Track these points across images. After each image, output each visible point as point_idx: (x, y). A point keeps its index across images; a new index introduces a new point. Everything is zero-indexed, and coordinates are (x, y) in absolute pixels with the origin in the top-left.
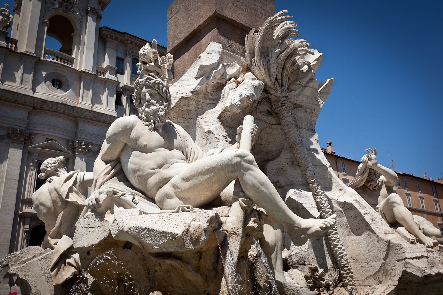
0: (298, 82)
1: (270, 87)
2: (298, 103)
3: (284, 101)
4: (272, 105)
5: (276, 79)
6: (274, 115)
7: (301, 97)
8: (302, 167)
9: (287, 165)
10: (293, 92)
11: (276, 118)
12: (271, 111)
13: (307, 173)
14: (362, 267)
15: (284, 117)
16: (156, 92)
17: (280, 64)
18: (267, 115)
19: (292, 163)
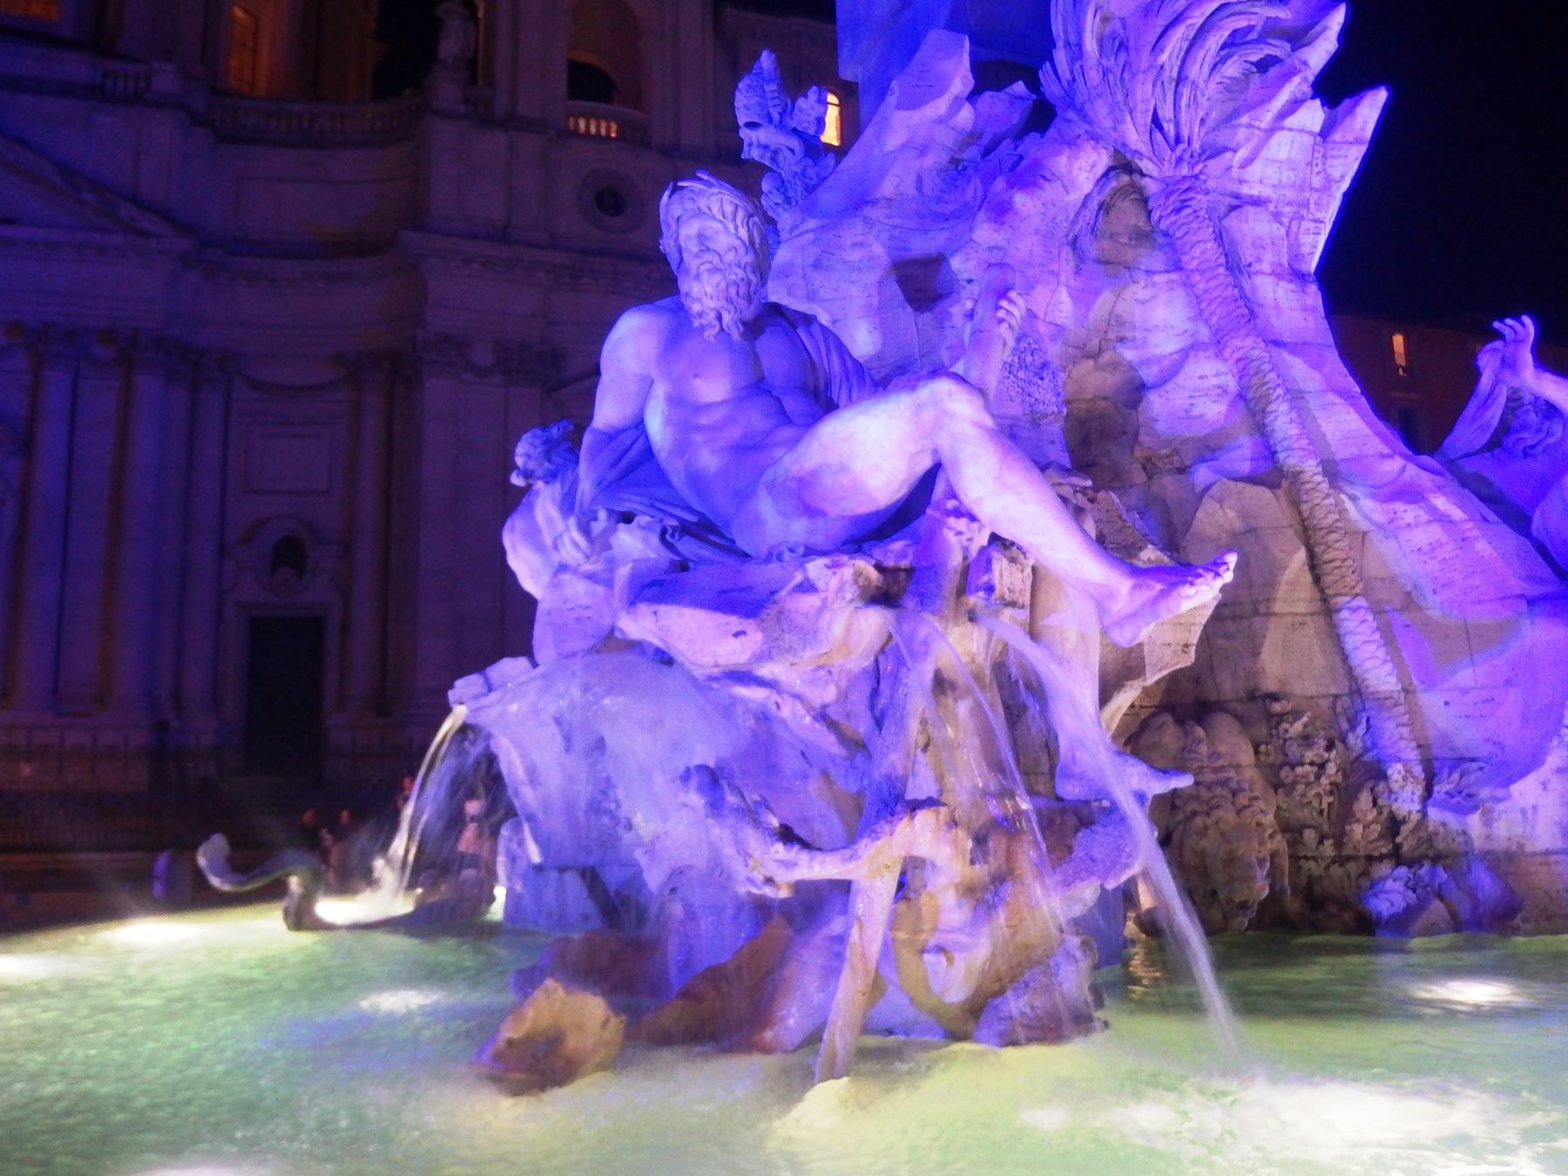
0: (1244, 120)
1: (1137, 152)
2: (1245, 190)
3: (1186, 190)
4: (1150, 208)
5: (1156, 121)
6: (1161, 240)
7: (1256, 169)
8: (1251, 400)
9: (1205, 399)
10: (1228, 155)
11: (1167, 249)
12: (1148, 229)
13: (1266, 421)
14: (1447, 704)
15: (1188, 246)
16: (718, 226)
17: (1167, 68)
18: (1133, 242)
19: (1220, 390)
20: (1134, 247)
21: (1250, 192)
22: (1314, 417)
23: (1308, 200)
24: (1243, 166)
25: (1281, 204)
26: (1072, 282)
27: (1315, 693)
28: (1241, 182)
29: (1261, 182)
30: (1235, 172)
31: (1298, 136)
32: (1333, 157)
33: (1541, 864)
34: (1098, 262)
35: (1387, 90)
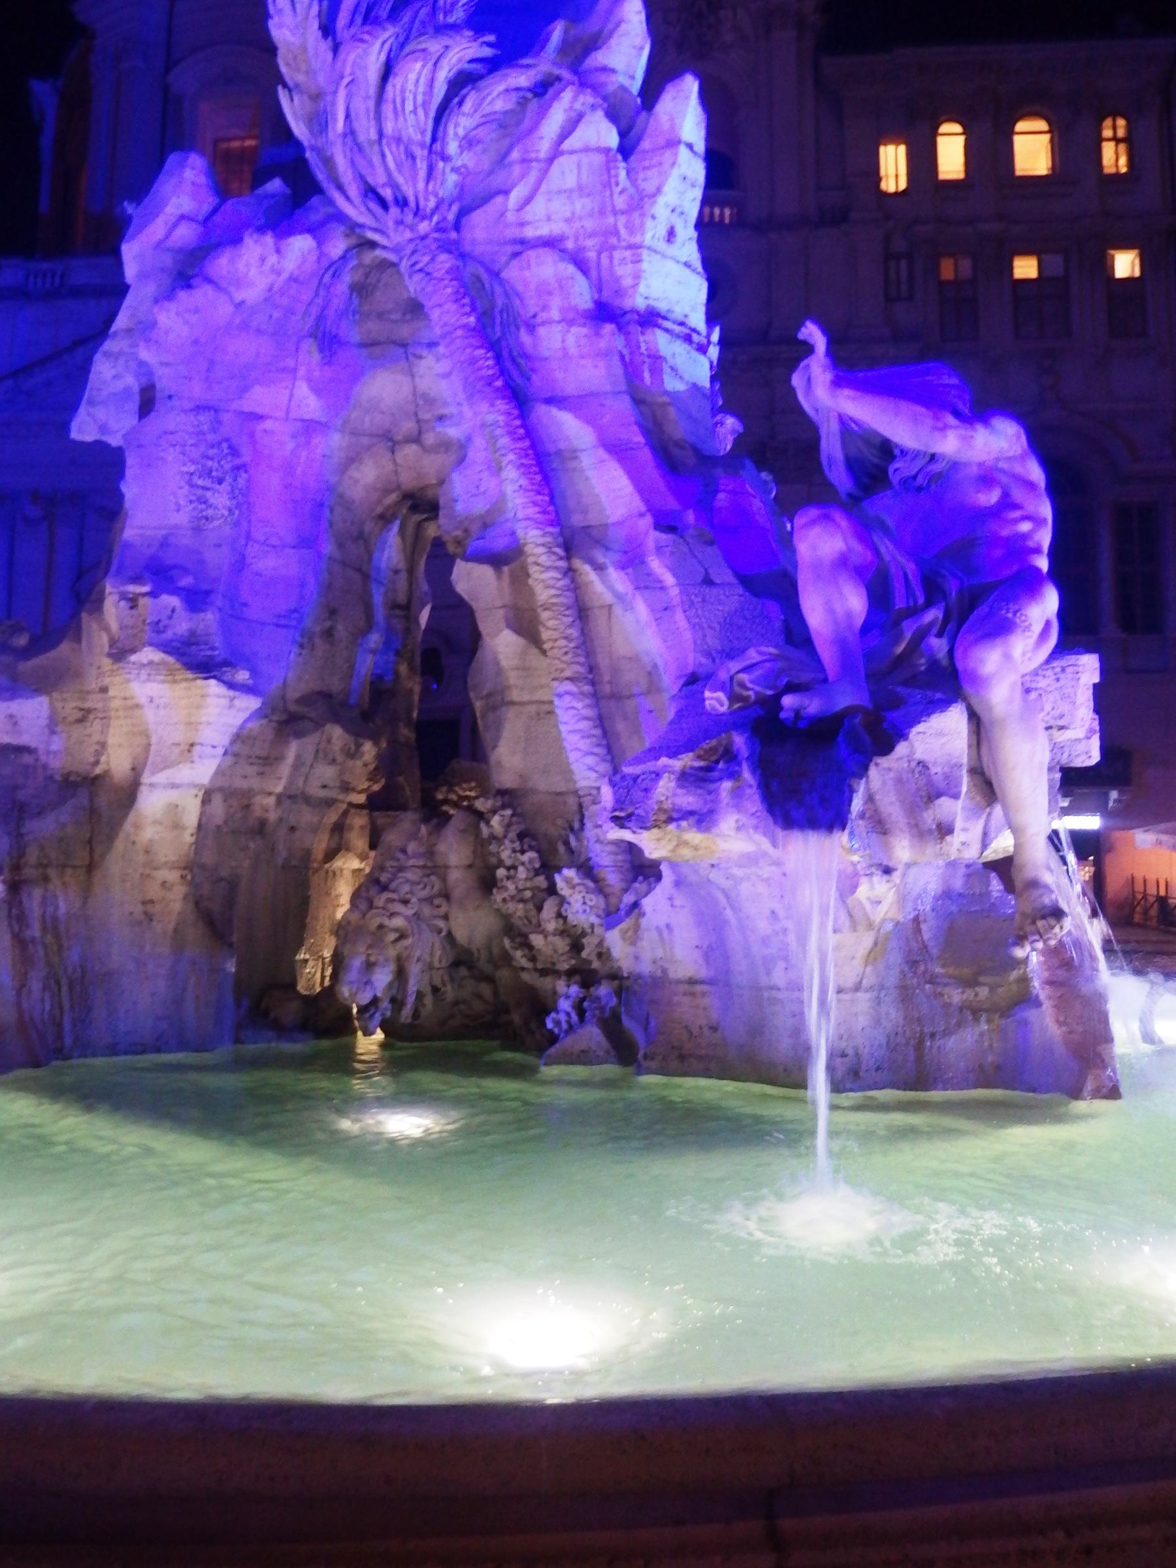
0: (515, 155)
2: (530, 233)
7: (538, 207)
10: (499, 199)
20: (412, 320)
21: (538, 233)
22: (587, 479)
23: (615, 225)
24: (520, 208)
25: (581, 237)
26: (317, 374)
27: (564, 790)
28: (522, 224)
29: (549, 219)
30: (510, 217)
31: (585, 159)
32: (645, 168)
33: (685, 994)
34: (363, 345)
35: (697, 75)
